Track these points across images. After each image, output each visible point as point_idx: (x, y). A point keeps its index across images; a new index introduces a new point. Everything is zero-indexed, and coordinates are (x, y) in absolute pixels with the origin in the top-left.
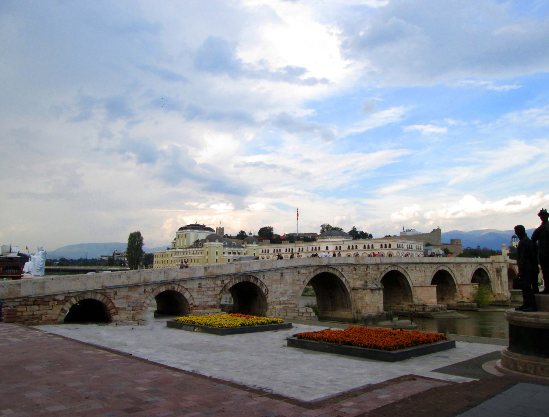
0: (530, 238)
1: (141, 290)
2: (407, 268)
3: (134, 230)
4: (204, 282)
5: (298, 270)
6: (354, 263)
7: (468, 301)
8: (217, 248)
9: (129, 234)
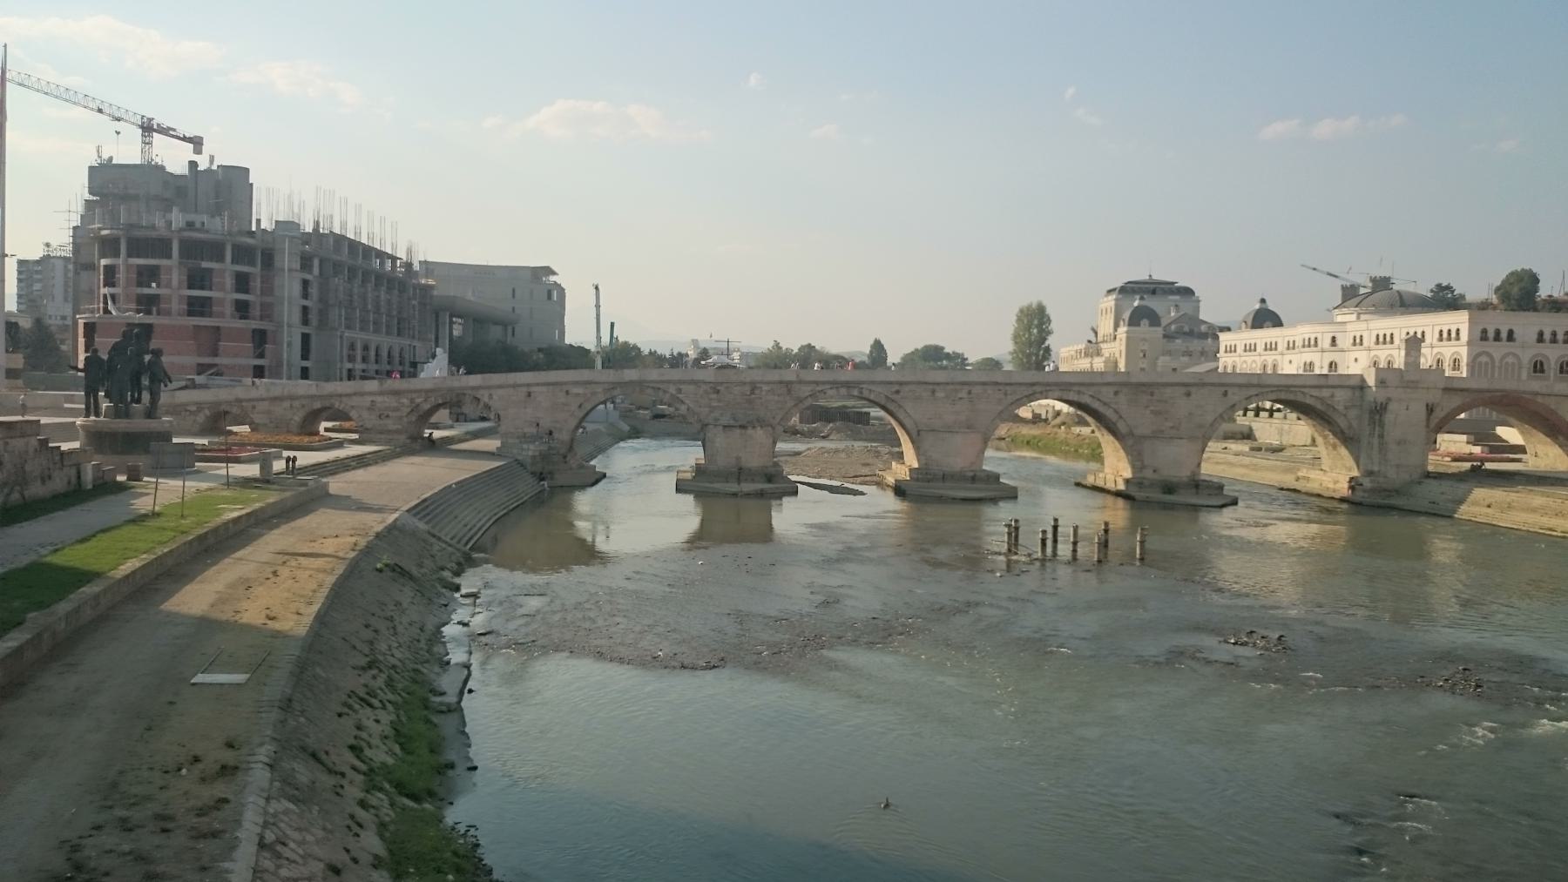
0: (105, 357)
1: (287, 404)
2: (898, 392)
3: (1032, 299)
4: (379, 399)
5: (565, 388)
6: (712, 379)
7: (1156, 476)
8: (1144, 340)
9: (1016, 310)
